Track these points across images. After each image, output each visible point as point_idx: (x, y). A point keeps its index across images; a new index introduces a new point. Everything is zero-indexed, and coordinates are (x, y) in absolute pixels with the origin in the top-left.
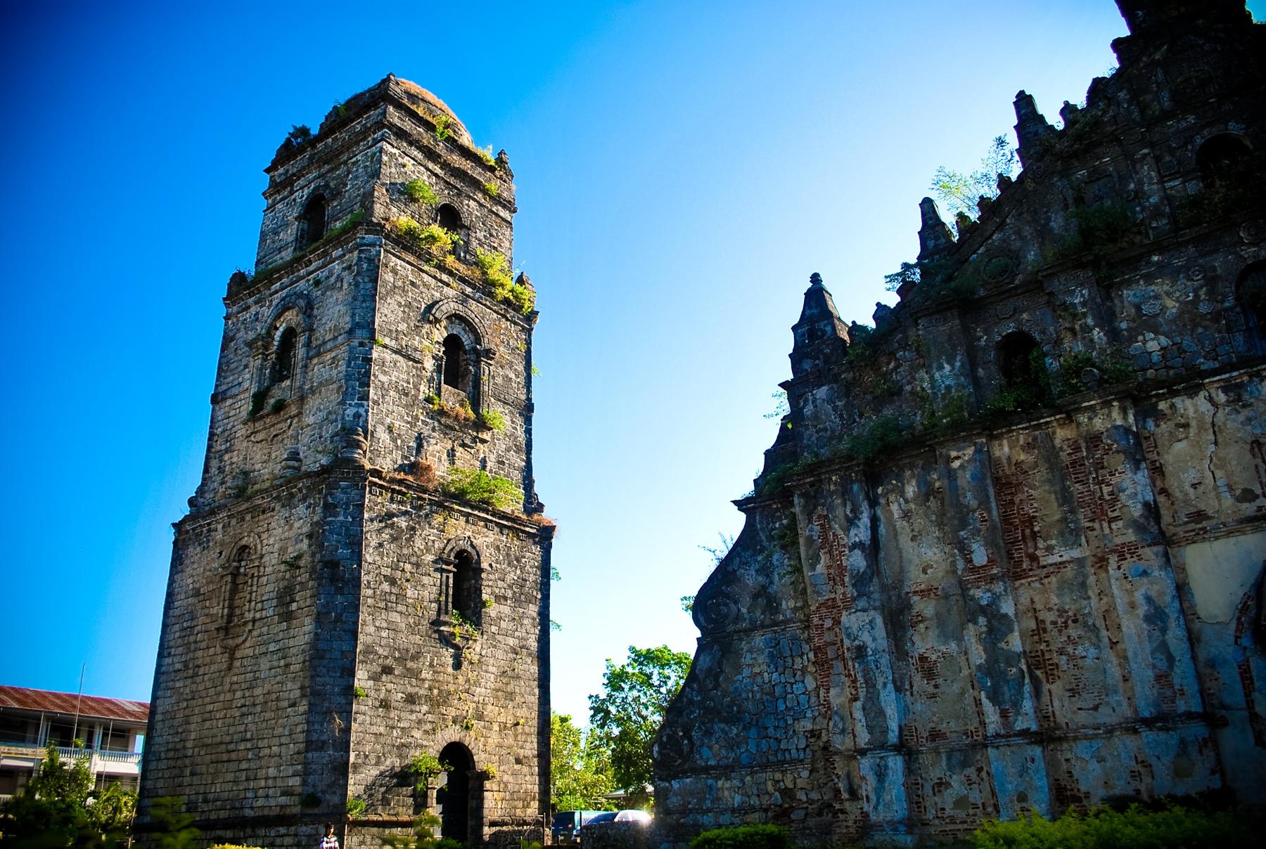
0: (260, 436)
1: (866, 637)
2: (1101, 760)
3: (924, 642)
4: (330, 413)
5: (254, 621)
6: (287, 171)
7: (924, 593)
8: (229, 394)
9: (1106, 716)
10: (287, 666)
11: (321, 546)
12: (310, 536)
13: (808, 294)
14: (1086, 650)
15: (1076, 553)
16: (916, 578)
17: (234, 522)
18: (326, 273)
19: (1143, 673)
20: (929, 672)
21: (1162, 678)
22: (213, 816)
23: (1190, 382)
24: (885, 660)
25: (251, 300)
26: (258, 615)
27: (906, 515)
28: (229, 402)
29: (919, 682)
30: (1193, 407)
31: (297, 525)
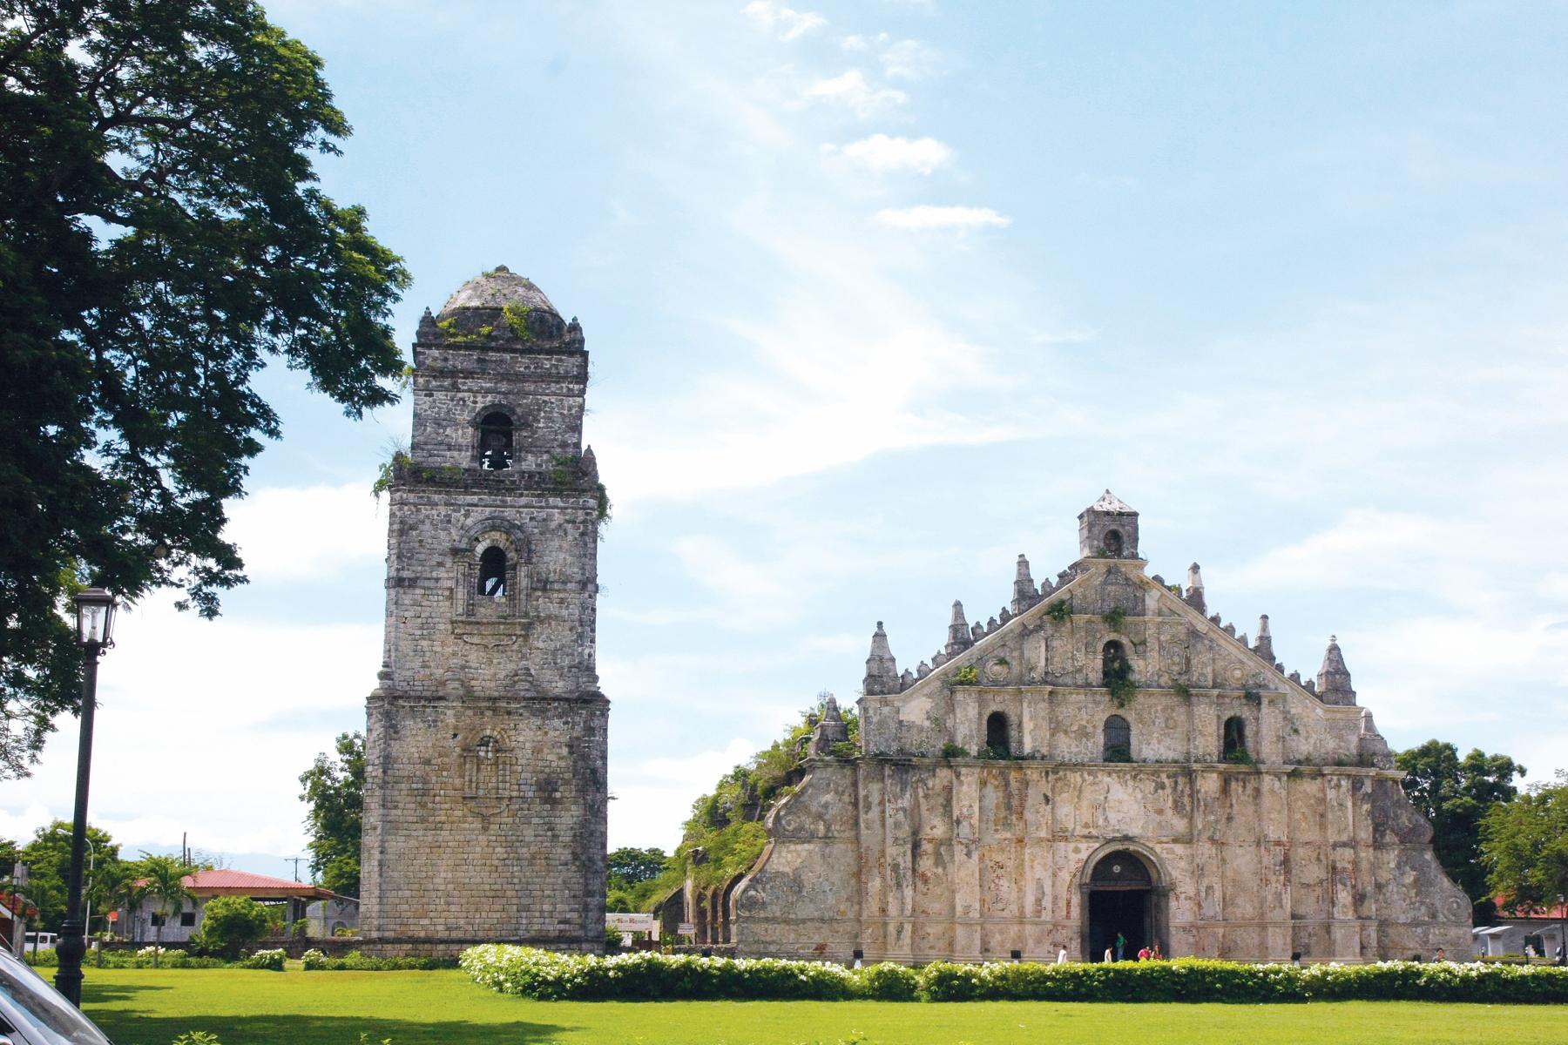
0: (476, 640)
1: (900, 860)
2: (1001, 933)
3: (926, 864)
4: (563, 646)
5: (511, 798)
6: (446, 360)
7: (930, 841)
8: (420, 583)
9: (1005, 914)
10: (555, 836)
11: (585, 757)
12: (570, 746)
13: (876, 635)
14: (1004, 883)
15: (1008, 835)
16: (927, 832)
17: (470, 713)
18: (543, 514)
19: (1030, 900)
20: (926, 881)
21: (1039, 901)
22: (480, 934)
23: (1077, 766)
24: (909, 873)
25: (436, 497)
26: (515, 794)
27: (926, 796)
28: (418, 591)
29: (920, 884)
30: (1074, 778)
31: (551, 734)
